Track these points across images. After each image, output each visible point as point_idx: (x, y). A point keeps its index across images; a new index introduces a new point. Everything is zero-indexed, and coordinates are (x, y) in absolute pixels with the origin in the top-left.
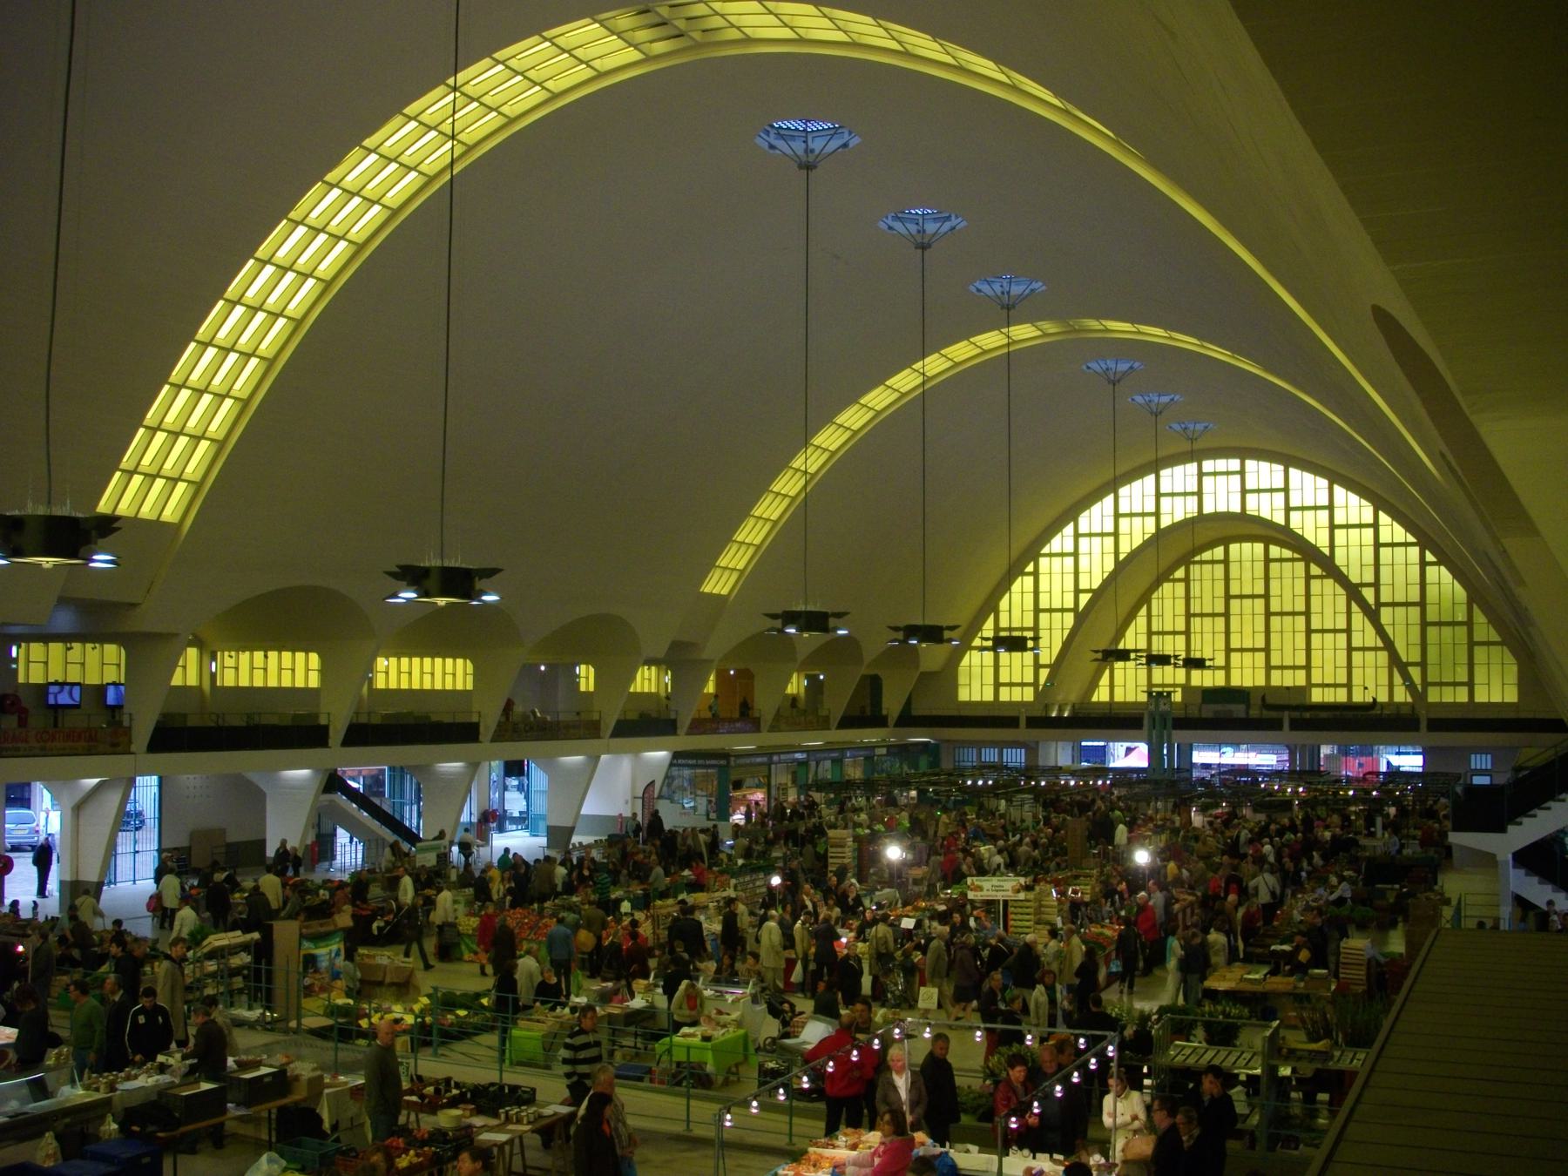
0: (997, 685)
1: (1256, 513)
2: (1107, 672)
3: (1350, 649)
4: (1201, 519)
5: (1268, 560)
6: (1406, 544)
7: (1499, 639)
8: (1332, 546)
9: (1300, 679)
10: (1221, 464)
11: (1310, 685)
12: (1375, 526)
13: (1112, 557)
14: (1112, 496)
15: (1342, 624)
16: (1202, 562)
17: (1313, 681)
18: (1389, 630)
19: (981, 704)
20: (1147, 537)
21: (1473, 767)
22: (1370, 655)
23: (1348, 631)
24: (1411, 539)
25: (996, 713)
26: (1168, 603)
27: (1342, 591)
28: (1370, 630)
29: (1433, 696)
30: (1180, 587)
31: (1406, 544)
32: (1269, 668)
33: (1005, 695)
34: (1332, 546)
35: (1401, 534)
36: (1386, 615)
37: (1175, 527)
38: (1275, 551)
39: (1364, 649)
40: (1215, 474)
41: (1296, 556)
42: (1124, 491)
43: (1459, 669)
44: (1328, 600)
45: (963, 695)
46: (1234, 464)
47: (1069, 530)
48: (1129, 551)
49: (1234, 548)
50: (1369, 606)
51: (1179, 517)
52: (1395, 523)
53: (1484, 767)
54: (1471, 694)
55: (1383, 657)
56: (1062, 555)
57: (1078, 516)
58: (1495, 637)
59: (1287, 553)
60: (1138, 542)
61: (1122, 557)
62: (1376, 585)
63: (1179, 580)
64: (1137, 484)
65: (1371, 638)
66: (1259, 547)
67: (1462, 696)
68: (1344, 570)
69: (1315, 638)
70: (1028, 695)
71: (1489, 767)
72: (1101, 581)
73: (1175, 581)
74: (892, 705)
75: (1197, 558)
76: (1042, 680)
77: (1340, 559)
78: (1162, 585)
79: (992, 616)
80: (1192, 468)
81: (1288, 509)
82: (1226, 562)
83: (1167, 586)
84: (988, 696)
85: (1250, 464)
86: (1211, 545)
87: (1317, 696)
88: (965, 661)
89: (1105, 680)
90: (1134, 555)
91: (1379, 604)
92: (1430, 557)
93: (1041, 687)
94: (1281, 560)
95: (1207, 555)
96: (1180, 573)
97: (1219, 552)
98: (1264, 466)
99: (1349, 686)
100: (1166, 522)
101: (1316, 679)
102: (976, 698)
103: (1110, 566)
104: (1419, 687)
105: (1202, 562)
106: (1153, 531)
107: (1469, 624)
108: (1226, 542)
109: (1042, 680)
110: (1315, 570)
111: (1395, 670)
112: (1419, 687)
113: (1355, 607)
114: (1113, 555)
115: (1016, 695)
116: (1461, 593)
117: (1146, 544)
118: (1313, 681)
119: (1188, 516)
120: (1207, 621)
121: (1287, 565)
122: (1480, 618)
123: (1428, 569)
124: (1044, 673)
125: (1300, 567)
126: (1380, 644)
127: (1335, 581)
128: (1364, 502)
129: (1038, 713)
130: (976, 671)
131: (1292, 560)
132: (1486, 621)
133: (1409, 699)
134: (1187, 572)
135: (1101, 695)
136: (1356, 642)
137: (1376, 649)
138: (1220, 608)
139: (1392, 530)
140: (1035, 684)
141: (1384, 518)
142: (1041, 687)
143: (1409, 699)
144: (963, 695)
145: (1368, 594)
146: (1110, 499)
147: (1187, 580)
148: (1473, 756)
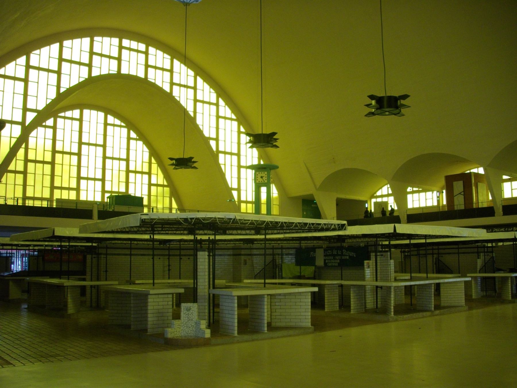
1: (153, 81)
4: (119, 76)
6: (231, 119)
10: (134, 44)
13: (55, 89)
14: (57, 45)
20: (81, 80)
24: (234, 117)
26: (41, 142)
30: (50, 131)
31: (231, 119)
37: (102, 78)
38: (111, 119)
40: (130, 49)
41: (123, 124)
42: (67, 43)
46: (142, 47)
47: (22, 60)
48: (68, 87)
49: (86, 112)
51: (105, 72)
52: (226, 106)
56: (14, 78)
57: (31, 52)
59: (118, 122)
60: (75, 82)
61: (62, 90)
64: (77, 41)
68: (201, 127)
72: (45, 105)
73: (46, 127)
75: (62, 114)
80: (115, 41)
83: (40, 129)
85: (152, 50)
86: (72, 107)
90: (70, 91)
91: (218, 152)
92: (242, 129)
94: (114, 125)
95: (68, 114)
96: (50, 122)
97: (76, 113)
98: (160, 53)
100: (95, 73)
103: (53, 95)
105: (65, 118)
106: (87, 77)
110: (133, 135)
114: (55, 88)
117: (81, 86)
119: (111, 72)
120: (66, 157)
121: (117, 129)
125: (125, 131)
128: (212, 90)
131: (121, 126)
138: (75, 150)
139: (225, 111)
141: (221, 102)
145: (213, 144)
146: (56, 47)
147: (54, 128)
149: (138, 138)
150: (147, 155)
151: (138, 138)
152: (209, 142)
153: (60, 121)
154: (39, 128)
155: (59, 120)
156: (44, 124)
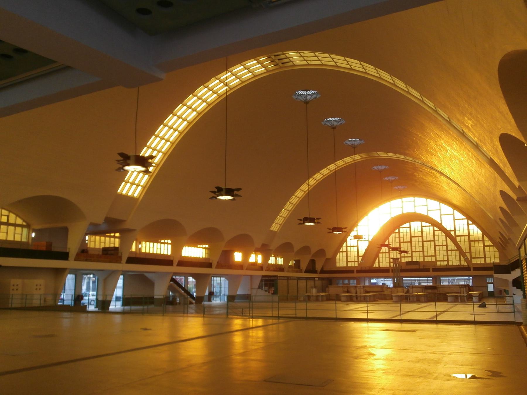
0: (347, 262)
2: (377, 259)
3: (447, 250)
5: (422, 227)
7: (493, 245)
8: (441, 221)
9: (433, 259)
11: (436, 261)
12: (453, 214)
15: (444, 243)
16: (403, 228)
17: (437, 260)
18: (459, 243)
19: (343, 267)
21: (487, 281)
22: (453, 252)
23: (447, 245)
25: (348, 269)
27: (443, 234)
28: (453, 245)
29: (474, 261)
32: (424, 256)
33: (349, 265)
34: (441, 221)
35: (461, 216)
36: (458, 239)
38: (424, 224)
39: (451, 250)
43: (481, 253)
44: (440, 237)
45: (338, 265)
49: (412, 223)
50: (453, 236)
53: (491, 281)
54: (485, 260)
55: (457, 252)
58: (491, 244)
62: (455, 231)
63: (397, 233)
65: (453, 247)
66: (420, 223)
67: (482, 261)
69: (437, 248)
70: (356, 264)
71: (492, 281)
74: (318, 267)
75: (402, 226)
76: (360, 260)
77: (444, 225)
78: (392, 234)
79: (345, 243)
81: (428, 210)
82: (410, 227)
84: (345, 265)
86: (405, 223)
87: (438, 264)
88: (338, 255)
89: (377, 261)
91: (456, 236)
92: (470, 222)
93: (360, 262)
94: (426, 226)
95: (404, 226)
96: (397, 231)
97: (407, 225)
99: (448, 261)
101: (438, 259)
102: (341, 266)
104: (469, 259)
105: (403, 228)
107: (483, 241)
108: (409, 221)
109: (360, 260)
110: (436, 229)
111: (461, 256)
112: (469, 259)
113: (448, 239)
115: (353, 264)
116: (480, 232)
118: (437, 260)
122: (486, 238)
123: (470, 226)
124: (360, 258)
126: (456, 249)
127: (442, 231)
129: (359, 269)
130: (341, 258)
131: (429, 226)
132: (488, 240)
133: (466, 264)
134: (399, 230)
135: (376, 265)
136: (449, 248)
137: (455, 250)
140: (358, 261)
141: (456, 212)
142: (360, 262)
143: (466, 264)
144: (338, 265)
145: (453, 233)
147: (399, 233)
148: (487, 278)
149: (438, 230)
150: (444, 237)
151: (438, 230)
152: (450, 233)
153: (401, 230)
154: (393, 234)
155: (400, 229)
156: (395, 232)
